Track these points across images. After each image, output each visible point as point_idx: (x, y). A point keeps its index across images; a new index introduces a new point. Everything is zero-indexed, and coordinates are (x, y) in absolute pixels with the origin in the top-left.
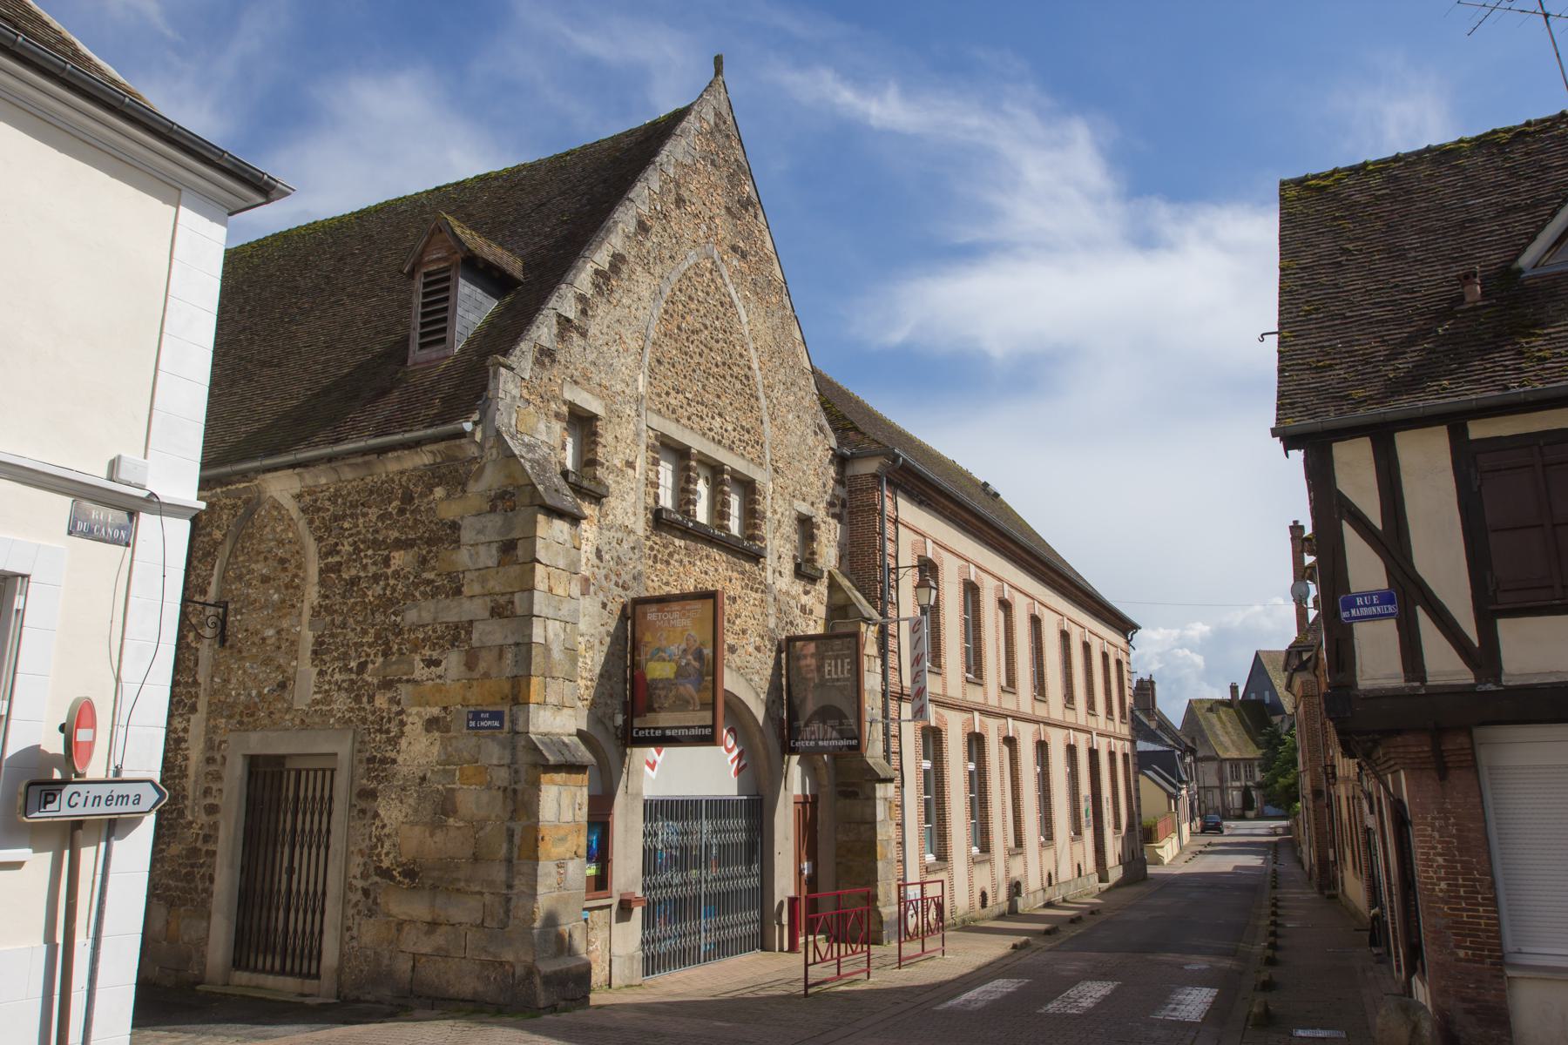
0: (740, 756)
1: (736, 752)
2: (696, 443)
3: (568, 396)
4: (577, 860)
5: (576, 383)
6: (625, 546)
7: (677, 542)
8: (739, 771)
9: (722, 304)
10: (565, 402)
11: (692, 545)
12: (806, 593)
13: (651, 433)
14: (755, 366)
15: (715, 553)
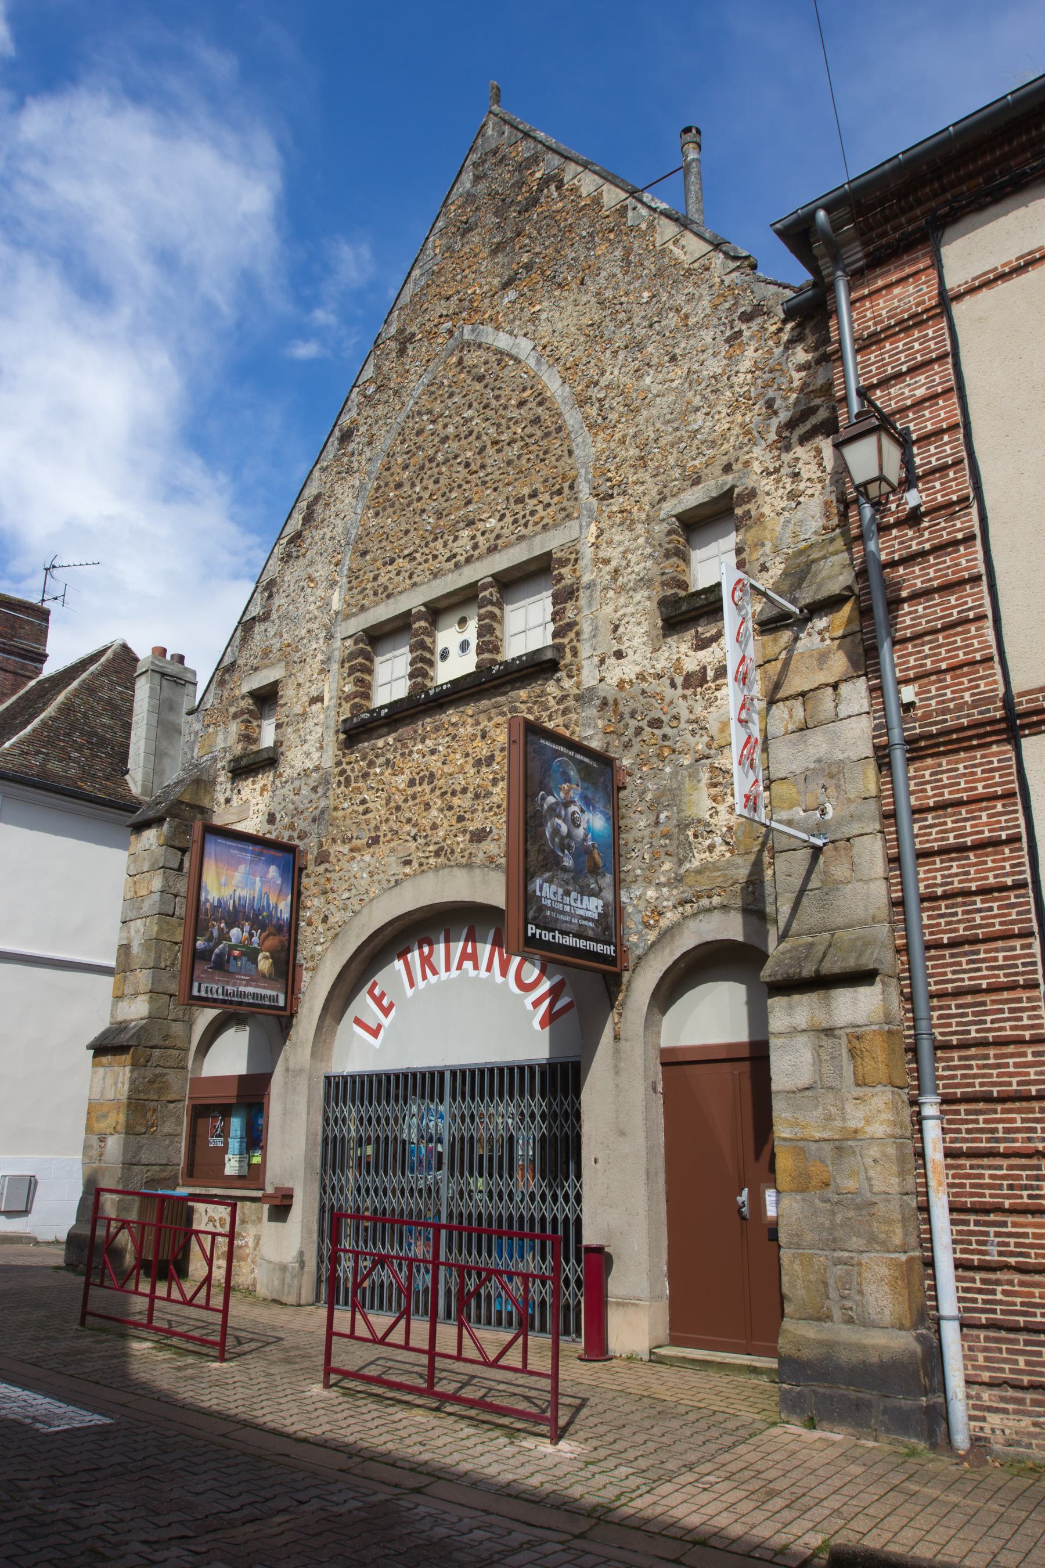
0: (555, 993)
1: (546, 986)
2: (413, 601)
3: (245, 689)
4: (117, 1136)
5: (256, 669)
6: (304, 792)
7: (380, 743)
8: (550, 1019)
9: (480, 379)
10: (243, 698)
11: (405, 731)
12: (702, 644)
13: (349, 642)
14: (553, 384)
15: (452, 715)
